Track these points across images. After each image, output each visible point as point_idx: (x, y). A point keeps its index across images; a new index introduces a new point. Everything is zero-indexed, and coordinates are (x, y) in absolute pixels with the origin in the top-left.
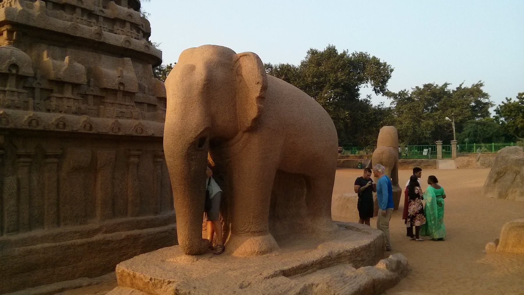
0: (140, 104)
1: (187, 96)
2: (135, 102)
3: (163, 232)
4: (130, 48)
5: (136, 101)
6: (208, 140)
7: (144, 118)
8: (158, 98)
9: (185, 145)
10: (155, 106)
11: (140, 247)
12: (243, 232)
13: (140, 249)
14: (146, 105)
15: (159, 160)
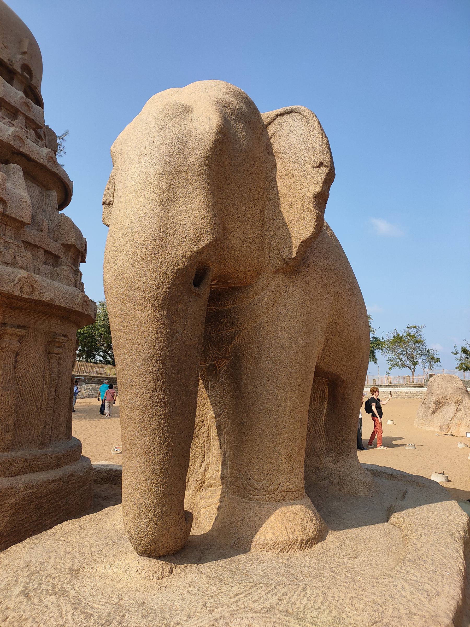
0: (31, 246)
1: (175, 160)
2: (23, 241)
3: (55, 481)
4: (22, 150)
5: (24, 239)
6: (211, 274)
7: (38, 272)
8: (63, 245)
9: (165, 273)
10: (57, 257)
11: (7, 514)
12: (262, 492)
13: (7, 519)
14: (42, 252)
15: (56, 350)
